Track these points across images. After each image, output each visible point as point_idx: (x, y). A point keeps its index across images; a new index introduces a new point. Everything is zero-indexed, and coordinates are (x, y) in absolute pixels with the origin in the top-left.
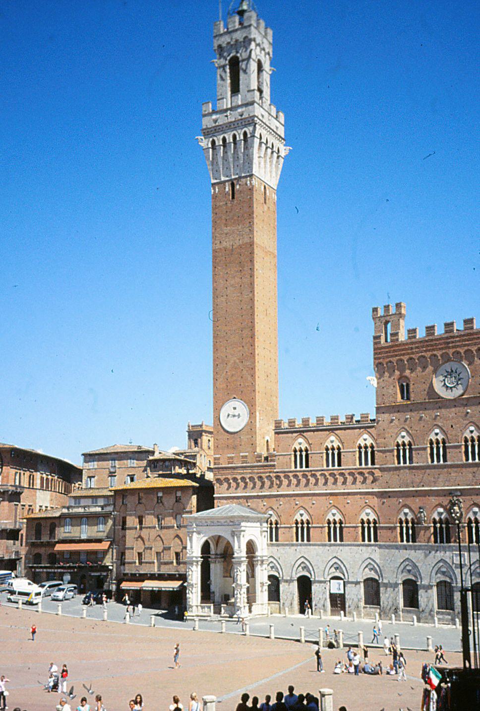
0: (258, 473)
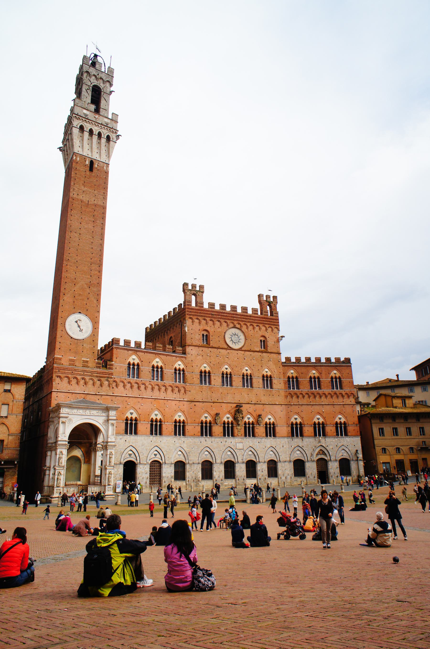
0: (97, 377)
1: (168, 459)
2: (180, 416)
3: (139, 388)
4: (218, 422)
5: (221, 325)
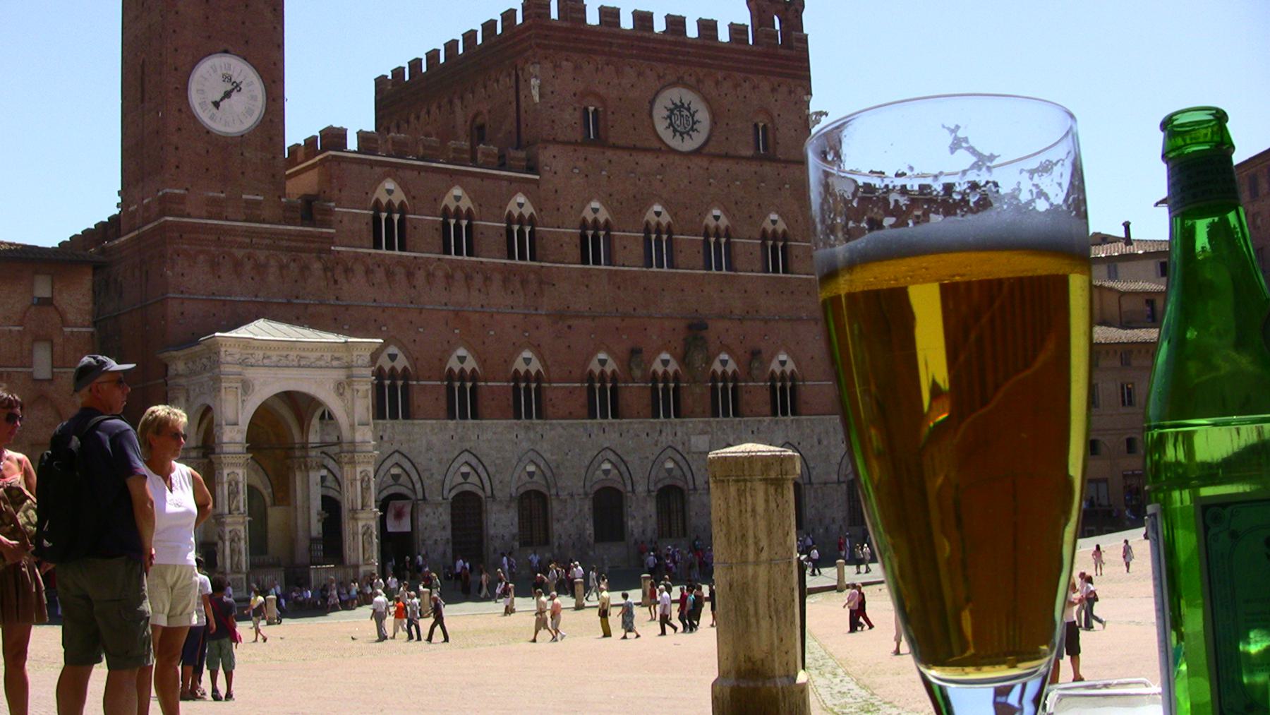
0: (289, 249)
1: (499, 487)
2: (527, 361)
3: (410, 275)
4: (637, 373)
5: (640, 74)
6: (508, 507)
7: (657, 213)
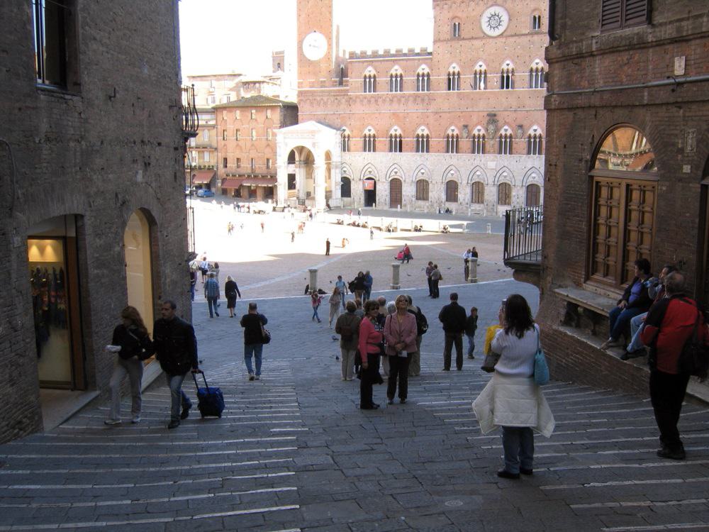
0: (334, 96)
2: (423, 130)
3: (376, 101)
6: (411, 185)
7: (481, 66)
